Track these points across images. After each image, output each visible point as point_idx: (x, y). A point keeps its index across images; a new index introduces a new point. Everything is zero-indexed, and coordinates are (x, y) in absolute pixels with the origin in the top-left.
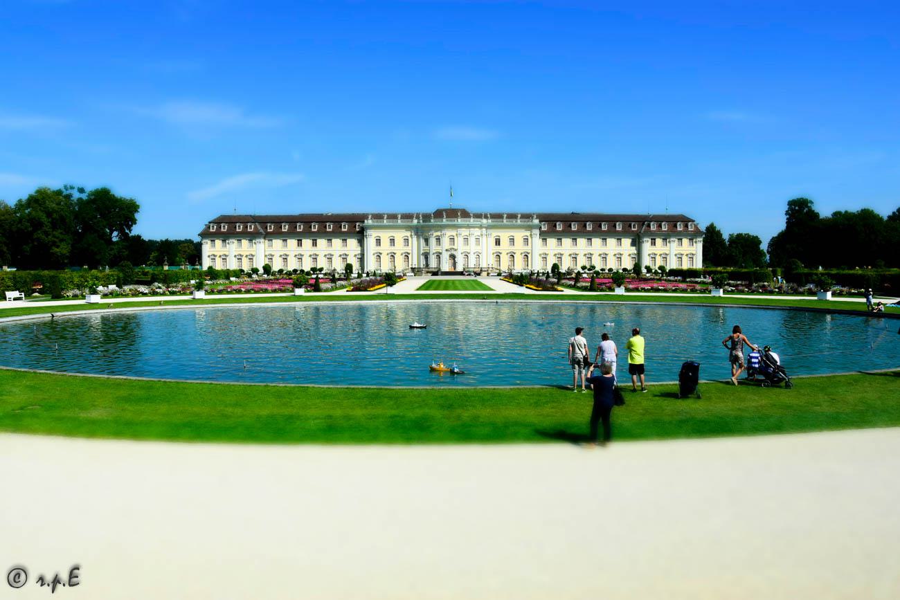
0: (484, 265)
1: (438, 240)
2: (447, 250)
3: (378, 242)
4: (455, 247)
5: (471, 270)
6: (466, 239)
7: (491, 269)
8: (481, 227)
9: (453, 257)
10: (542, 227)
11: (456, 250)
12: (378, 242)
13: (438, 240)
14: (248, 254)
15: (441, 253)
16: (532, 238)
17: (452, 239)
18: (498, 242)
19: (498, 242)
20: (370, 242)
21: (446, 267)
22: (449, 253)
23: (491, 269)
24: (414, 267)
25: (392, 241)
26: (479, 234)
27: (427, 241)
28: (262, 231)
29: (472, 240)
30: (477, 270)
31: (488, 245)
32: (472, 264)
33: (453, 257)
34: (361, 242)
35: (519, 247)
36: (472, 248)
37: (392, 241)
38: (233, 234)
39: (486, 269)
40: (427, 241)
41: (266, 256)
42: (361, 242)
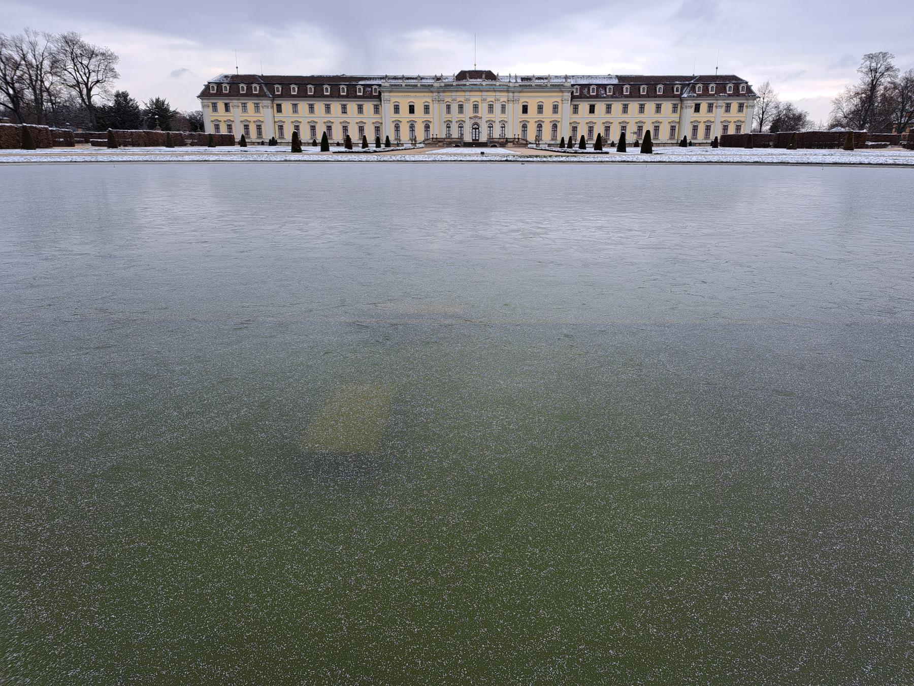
0: (510, 135)
1: (461, 107)
2: (470, 118)
3: (397, 109)
4: (479, 115)
5: (496, 140)
6: (491, 107)
7: (517, 140)
8: (508, 91)
9: (476, 127)
10: (575, 91)
11: (481, 118)
12: (397, 109)
13: (461, 107)
14: (256, 119)
15: (464, 122)
16: (562, 103)
17: (476, 107)
18: (525, 110)
19: (525, 110)
20: (387, 108)
21: (468, 138)
22: (473, 122)
23: (517, 140)
24: (435, 137)
25: (412, 109)
26: (505, 100)
27: (448, 107)
28: (268, 93)
29: (497, 107)
30: (502, 140)
31: (514, 113)
32: (496, 134)
33: (476, 127)
34: (377, 109)
35: (548, 115)
36: (497, 115)
37: (412, 109)
38: (237, 96)
39: (511, 140)
40: (448, 107)
41: (275, 122)
42: (377, 109)
